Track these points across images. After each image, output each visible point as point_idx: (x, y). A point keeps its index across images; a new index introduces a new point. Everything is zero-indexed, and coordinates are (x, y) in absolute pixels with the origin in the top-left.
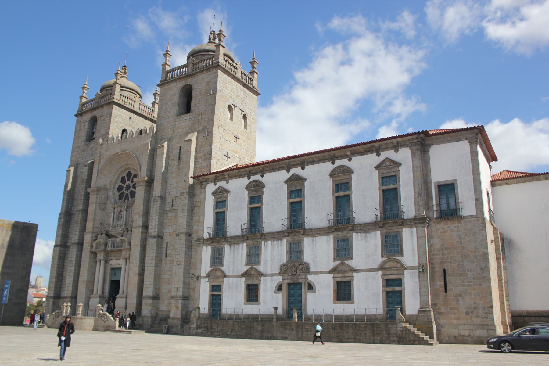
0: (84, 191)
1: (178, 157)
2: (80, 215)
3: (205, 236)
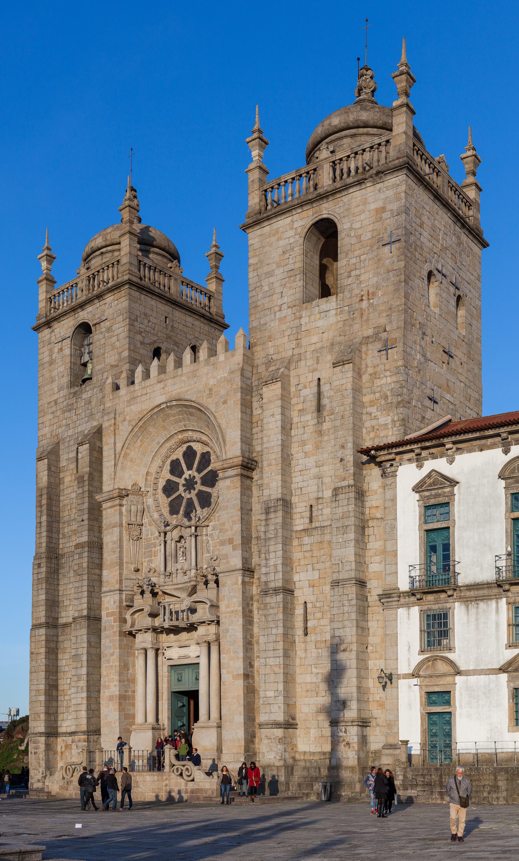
1: (314, 403)
3: (404, 585)
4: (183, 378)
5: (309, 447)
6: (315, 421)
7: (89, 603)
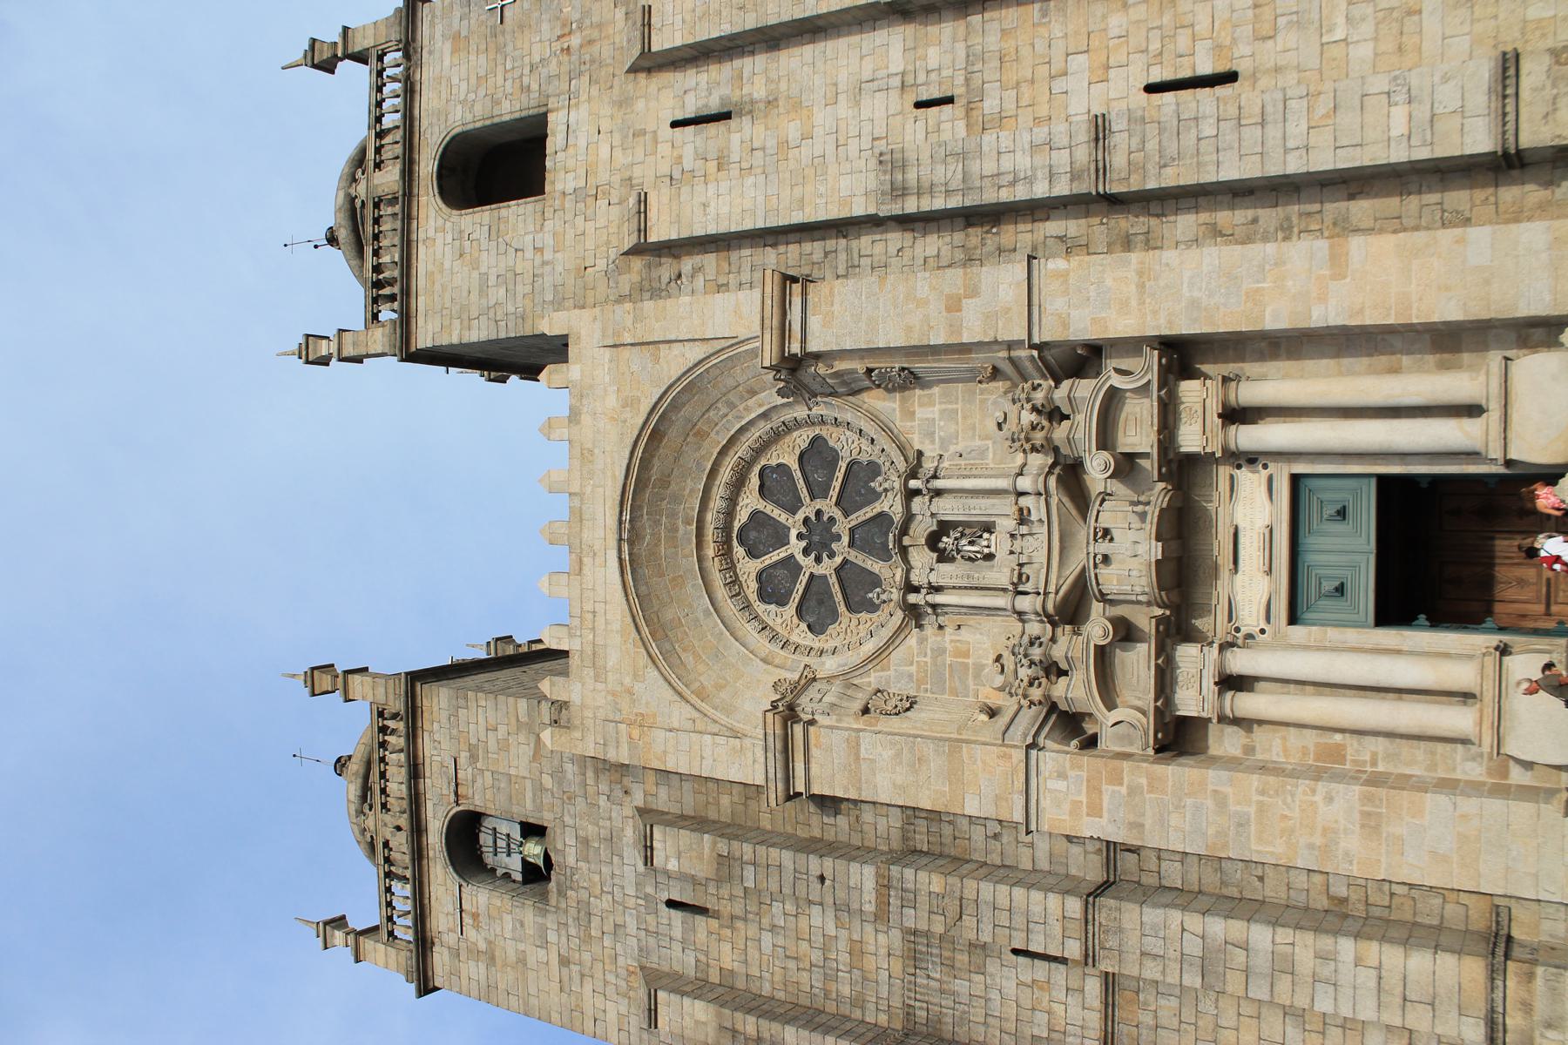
0: (774, 852)
2: (909, 873)
4: (588, 490)
5: (793, 130)
6: (746, 120)
7: (1048, 890)
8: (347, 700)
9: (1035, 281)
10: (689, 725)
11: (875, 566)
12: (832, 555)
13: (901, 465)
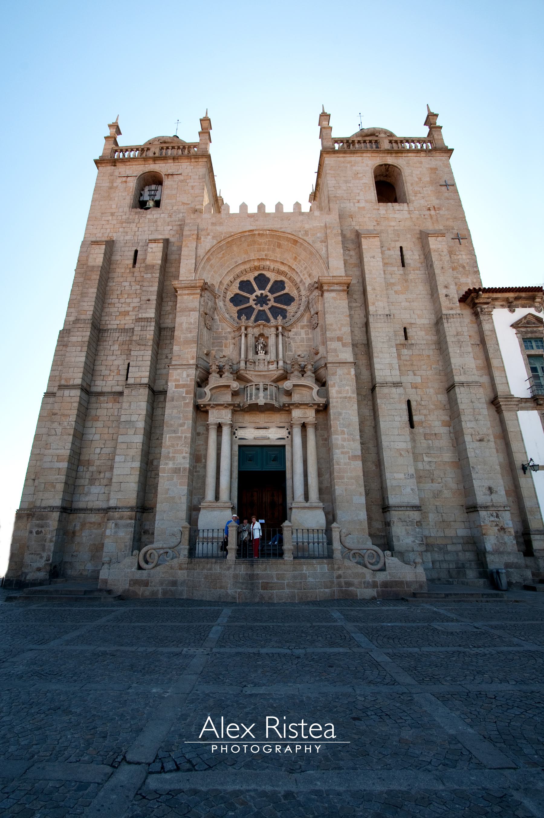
0: (157, 284)
2: (153, 328)
4: (276, 219)
6: (401, 272)
8: (199, 133)
9: (347, 365)
10: (198, 255)
11: (253, 318)
12: (256, 304)
13: (286, 325)
